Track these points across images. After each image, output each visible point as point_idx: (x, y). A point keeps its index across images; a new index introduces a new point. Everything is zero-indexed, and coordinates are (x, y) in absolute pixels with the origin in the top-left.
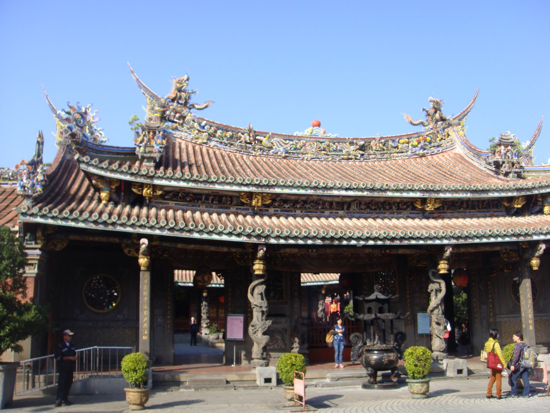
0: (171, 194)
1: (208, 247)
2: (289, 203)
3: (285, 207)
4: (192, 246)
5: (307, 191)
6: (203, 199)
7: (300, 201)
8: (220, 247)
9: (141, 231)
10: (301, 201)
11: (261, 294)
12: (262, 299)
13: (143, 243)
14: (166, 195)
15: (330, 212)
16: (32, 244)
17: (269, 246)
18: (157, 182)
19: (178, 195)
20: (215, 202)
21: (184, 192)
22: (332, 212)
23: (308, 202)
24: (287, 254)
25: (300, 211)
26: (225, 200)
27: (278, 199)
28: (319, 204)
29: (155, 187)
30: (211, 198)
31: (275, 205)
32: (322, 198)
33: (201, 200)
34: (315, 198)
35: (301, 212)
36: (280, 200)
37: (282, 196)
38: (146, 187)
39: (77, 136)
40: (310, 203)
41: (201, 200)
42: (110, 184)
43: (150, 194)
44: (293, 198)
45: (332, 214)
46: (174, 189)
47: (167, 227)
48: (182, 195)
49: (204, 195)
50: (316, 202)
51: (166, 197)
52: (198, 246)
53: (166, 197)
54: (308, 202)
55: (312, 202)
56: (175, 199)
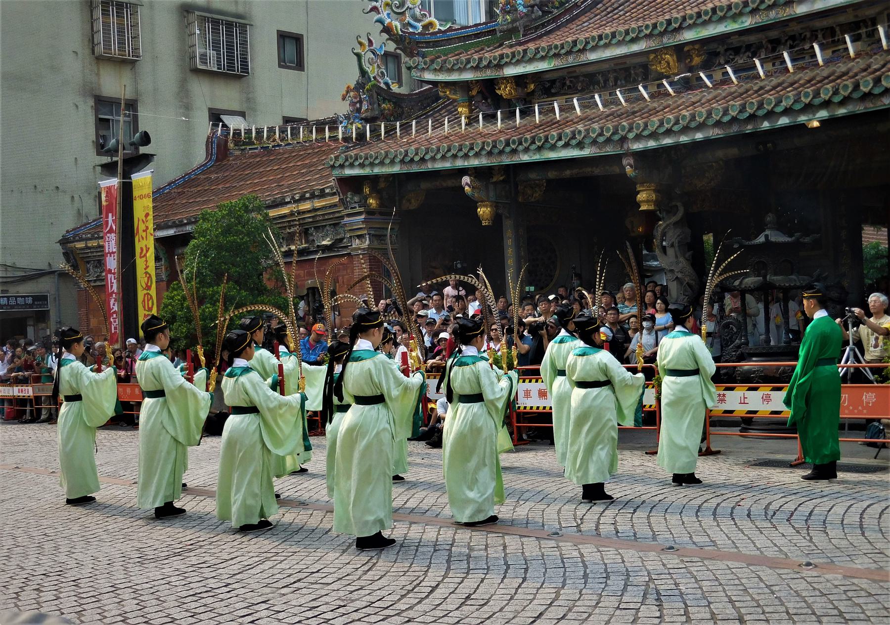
0: (558, 84)
1: (590, 170)
2: (745, 52)
3: (737, 62)
5: (742, 22)
7: (764, 42)
8: (607, 167)
9: (460, 163)
10: (771, 41)
11: (672, 245)
12: (677, 257)
13: (467, 184)
14: (551, 87)
15: (834, 52)
16: (355, 207)
17: (641, 156)
18: (511, 71)
19: (564, 84)
20: (619, 82)
21: (574, 75)
23: (783, 41)
24: (721, 163)
25: (771, 64)
26: (635, 73)
27: (721, 49)
29: (519, 80)
30: (611, 77)
33: (598, 83)
34: (795, 28)
35: (774, 65)
36: (726, 50)
38: (503, 83)
40: (786, 41)
41: (598, 83)
43: (510, 93)
44: (752, 39)
45: (836, 54)
46: (560, 74)
47: (484, 152)
48: (571, 81)
49: (599, 73)
50: (801, 34)
51: (553, 91)
52: (575, 171)
53: (553, 91)
54: (783, 41)
55: (793, 38)
56: (562, 92)
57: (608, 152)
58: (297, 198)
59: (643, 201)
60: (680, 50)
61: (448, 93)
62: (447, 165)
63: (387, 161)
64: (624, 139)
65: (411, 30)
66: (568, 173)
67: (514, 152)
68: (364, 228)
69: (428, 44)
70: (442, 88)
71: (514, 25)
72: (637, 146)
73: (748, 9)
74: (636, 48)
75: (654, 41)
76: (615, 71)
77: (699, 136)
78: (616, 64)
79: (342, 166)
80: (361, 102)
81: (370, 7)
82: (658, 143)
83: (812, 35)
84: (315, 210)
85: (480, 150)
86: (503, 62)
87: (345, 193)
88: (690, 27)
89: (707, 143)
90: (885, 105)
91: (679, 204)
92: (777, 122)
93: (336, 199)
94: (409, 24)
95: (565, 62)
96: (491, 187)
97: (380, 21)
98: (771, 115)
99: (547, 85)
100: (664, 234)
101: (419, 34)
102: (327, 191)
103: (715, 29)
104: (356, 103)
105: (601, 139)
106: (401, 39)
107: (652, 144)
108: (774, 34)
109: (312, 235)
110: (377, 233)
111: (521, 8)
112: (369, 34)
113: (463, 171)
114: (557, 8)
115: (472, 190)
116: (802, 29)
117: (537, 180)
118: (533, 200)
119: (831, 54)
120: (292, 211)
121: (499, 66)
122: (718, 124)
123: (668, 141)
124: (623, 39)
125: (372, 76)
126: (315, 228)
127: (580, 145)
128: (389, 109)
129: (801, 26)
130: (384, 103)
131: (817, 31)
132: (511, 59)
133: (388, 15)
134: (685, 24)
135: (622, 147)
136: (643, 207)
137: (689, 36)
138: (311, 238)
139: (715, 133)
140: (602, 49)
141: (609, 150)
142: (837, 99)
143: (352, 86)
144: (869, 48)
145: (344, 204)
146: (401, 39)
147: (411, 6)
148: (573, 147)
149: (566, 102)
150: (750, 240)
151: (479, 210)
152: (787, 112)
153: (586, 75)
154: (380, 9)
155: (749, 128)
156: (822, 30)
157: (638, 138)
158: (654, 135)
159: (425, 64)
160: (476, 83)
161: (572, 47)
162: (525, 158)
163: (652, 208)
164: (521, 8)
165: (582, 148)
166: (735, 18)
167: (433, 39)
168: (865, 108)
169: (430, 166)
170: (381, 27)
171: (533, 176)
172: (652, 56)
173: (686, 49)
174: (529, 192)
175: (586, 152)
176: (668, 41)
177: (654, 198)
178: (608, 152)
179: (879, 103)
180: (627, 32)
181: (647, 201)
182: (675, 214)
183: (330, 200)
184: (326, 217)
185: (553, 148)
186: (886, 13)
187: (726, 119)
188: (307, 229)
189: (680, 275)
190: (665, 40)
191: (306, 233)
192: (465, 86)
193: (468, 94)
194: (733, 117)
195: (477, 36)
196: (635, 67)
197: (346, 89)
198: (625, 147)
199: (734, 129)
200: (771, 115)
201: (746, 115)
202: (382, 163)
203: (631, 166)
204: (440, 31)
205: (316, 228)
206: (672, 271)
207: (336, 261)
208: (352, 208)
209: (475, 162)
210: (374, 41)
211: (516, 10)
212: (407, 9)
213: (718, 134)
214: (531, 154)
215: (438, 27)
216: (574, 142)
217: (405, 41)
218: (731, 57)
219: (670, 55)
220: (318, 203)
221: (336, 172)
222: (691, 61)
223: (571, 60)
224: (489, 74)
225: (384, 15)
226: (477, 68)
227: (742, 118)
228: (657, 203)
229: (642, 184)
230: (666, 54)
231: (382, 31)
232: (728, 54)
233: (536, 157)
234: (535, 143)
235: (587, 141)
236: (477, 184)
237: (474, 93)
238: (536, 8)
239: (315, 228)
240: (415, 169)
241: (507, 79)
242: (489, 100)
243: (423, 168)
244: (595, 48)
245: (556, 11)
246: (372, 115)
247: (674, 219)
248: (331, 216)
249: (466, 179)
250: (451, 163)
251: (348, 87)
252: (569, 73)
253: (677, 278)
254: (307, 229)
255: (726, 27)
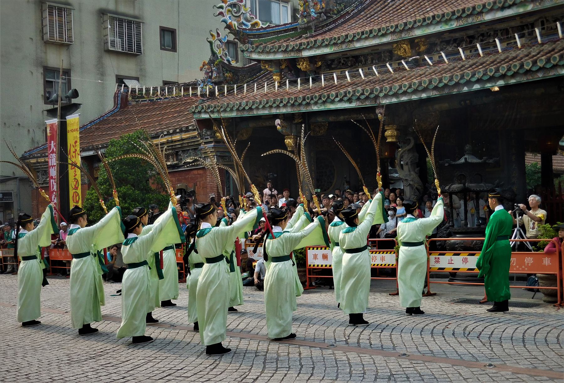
0: (336, 62)
2: (452, 44)
4: (342, 118)
5: (451, 25)
6: (363, 61)
7: (465, 37)
9: (274, 111)
11: (407, 164)
12: (409, 171)
13: (278, 124)
14: (332, 64)
15: (508, 44)
16: (208, 138)
19: (340, 62)
20: (374, 62)
22: (511, 43)
23: (477, 36)
24: (438, 112)
27: (438, 41)
28: (490, 36)
29: (312, 59)
30: (369, 58)
31: (437, 50)
32: (494, 26)
33: (361, 62)
34: (484, 29)
35: (471, 52)
36: (441, 42)
37: (443, 36)
38: (301, 61)
39: (232, 27)
42: (280, 66)
43: (306, 68)
44: (457, 35)
45: (509, 46)
47: (289, 105)
48: (344, 60)
49: (362, 56)
50: (487, 33)
51: (333, 66)
55: (483, 35)
56: (339, 67)
57: (367, 105)
58: (171, 132)
59: (389, 136)
60: (412, 42)
61: (267, 67)
62: (266, 112)
63: (228, 109)
64: (377, 97)
65: (244, 27)
66: (342, 118)
67: (308, 104)
68: (214, 151)
69: (255, 36)
70: (263, 64)
71: (309, 25)
72: (385, 101)
73: (455, 17)
74: (385, 40)
75: (396, 35)
76: (372, 54)
77: (424, 96)
78: (372, 50)
79: (200, 112)
80: (212, 72)
81: (218, 12)
82: (398, 100)
83: (494, 34)
84: (182, 140)
85: (287, 103)
86: (302, 48)
87: (201, 129)
88: (419, 27)
89: (429, 100)
90: (539, 78)
91: (411, 138)
92: (473, 87)
93: (196, 133)
94: (243, 23)
95: (340, 48)
96: (294, 126)
97: (224, 21)
98: (469, 83)
99: (329, 62)
100: (402, 157)
101: (249, 30)
102: (190, 128)
103: (434, 29)
104: (209, 73)
105: (363, 97)
106: (238, 33)
107: (394, 100)
108: (471, 32)
109: (180, 155)
110: (222, 155)
111: (313, 14)
112: (217, 29)
113: (276, 116)
114: (336, 14)
115: (282, 128)
116: (488, 29)
117: (323, 122)
118: (320, 134)
119: (506, 45)
120: (168, 140)
121: (299, 51)
122: (436, 88)
123: (404, 98)
124: (377, 35)
125: (219, 56)
126: (182, 151)
127: (350, 101)
128: (230, 77)
129: (488, 27)
130: (226, 73)
131: (497, 31)
132: (307, 46)
133: (230, 17)
134: (416, 26)
135: (376, 102)
136: (389, 140)
137: (418, 33)
138: (180, 157)
139: (433, 94)
140: (364, 40)
141: (368, 104)
142: (509, 74)
143: (207, 62)
144: (530, 42)
145: (201, 136)
146: (238, 33)
147: (244, 12)
148: (345, 102)
149: (341, 73)
150: (455, 161)
151: (286, 140)
152: (479, 81)
153: (353, 57)
154: (224, 13)
155: (455, 91)
156: (501, 30)
157: (386, 96)
158: (396, 95)
159: (253, 48)
160: (284, 61)
161: (345, 39)
162: (315, 108)
163: (394, 140)
164: (313, 14)
165: (351, 102)
166: (447, 22)
167: (258, 33)
168: (527, 79)
169: (255, 113)
170: (225, 25)
171: (320, 119)
172: (395, 46)
173: (416, 41)
174: (317, 129)
175: (353, 105)
176: (405, 36)
177: (396, 134)
178: (367, 105)
179: (536, 76)
180: (379, 30)
181: (391, 136)
182: (408, 144)
183: (192, 134)
184: (190, 144)
185: (333, 102)
186: (540, 20)
187: (441, 85)
188: (177, 152)
189: (411, 183)
190: (403, 35)
191: (177, 154)
192: (278, 63)
193: (280, 68)
194: (445, 84)
195: (285, 31)
196: (384, 52)
197: (202, 64)
198: (378, 102)
199: (446, 91)
200: (469, 83)
201: (453, 83)
202: (225, 111)
203: (381, 114)
204: (262, 28)
205: (184, 151)
206: (406, 180)
207: (196, 172)
208: (206, 139)
209: (283, 111)
210: (220, 34)
211: (310, 15)
212: (241, 14)
213: (435, 95)
214: (318, 106)
215: (261, 25)
216: (346, 99)
217: (240, 34)
218: (444, 46)
219: (407, 45)
220: (184, 136)
221: (196, 116)
222: (419, 49)
223: (344, 47)
224: (292, 55)
225: (227, 17)
226: (285, 51)
227: (451, 85)
228: (397, 137)
229: (388, 125)
230: (404, 44)
231: (226, 28)
232: (442, 44)
233: (322, 108)
234: (321, 99)
235: (354, 98)
236: (285, 124)
237: (283, 67)
238: (322, 14)
239: (182, 151)
240: (246, 114)
241: (304, 59)
242: (293, 72)
243: (251, 114)
244: (359, 40)
245: (335, 16)
246: (219, 80)
247: (408, 147)
248: (193, 144)
249: (278, 121)
250: (269, 111)
251: (204, 63)
252: (343, 55)
253: (410, 184)
254: (177, 152)
255: (441, 27)
